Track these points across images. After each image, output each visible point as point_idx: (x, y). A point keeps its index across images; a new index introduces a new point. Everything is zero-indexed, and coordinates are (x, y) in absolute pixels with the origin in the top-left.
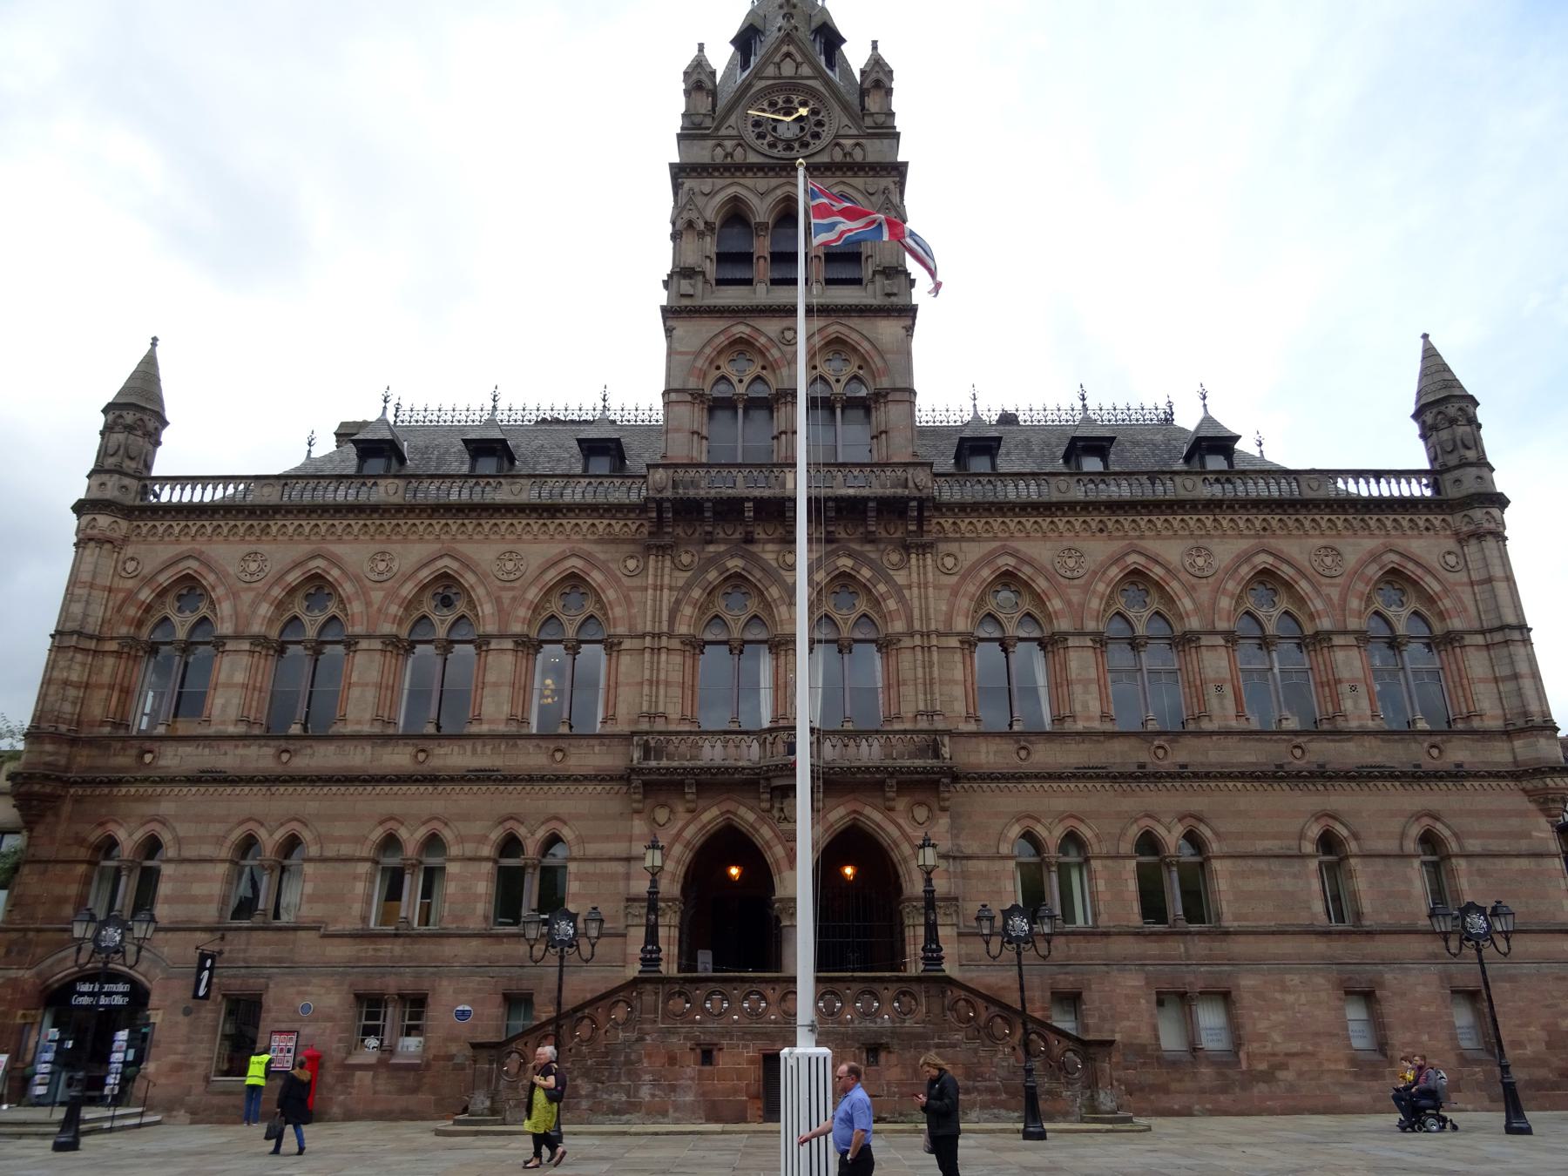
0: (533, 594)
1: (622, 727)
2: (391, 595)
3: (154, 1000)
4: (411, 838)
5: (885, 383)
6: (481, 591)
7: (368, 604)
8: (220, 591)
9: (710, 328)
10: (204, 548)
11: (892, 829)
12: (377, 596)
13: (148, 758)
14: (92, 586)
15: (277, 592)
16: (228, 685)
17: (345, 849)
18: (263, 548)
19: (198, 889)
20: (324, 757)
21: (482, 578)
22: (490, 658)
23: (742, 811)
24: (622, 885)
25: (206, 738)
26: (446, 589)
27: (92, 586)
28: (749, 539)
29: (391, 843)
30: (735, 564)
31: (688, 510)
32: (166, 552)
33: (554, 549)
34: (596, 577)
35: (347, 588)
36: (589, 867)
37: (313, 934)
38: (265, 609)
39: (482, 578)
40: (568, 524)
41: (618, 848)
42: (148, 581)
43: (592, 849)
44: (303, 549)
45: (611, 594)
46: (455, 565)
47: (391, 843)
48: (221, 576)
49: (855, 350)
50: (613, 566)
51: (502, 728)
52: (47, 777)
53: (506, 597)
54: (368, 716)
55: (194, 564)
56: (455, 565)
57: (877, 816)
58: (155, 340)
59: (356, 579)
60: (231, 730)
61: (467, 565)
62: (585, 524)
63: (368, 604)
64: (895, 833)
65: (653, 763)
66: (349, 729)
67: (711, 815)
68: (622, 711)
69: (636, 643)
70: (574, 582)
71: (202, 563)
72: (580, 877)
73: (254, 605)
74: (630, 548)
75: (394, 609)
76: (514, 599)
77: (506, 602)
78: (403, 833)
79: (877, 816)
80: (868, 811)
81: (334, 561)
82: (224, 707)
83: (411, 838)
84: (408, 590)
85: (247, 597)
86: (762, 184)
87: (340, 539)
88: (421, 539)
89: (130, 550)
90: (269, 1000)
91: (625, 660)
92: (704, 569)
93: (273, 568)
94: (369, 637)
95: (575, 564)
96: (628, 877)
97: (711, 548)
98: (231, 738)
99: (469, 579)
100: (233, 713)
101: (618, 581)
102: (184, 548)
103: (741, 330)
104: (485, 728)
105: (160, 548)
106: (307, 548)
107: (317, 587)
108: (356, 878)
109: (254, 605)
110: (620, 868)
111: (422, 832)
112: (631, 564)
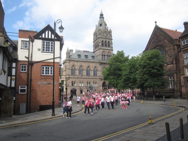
3: (77, 90)
4: (89, 82)
26: (88, 67)
29: (88, 82)
31: (102, 63)
38: (79, 67)
41: (99, 82)
44: (80, 64)
47: (88, 82)
67: (104, 81)
68: (99, 75)
70: (96, 67)
83: (89, 82)
86: (105, 39)
89: (70, 63)
100: (78, 74)
103: (104, 51)
107: (81, 66)
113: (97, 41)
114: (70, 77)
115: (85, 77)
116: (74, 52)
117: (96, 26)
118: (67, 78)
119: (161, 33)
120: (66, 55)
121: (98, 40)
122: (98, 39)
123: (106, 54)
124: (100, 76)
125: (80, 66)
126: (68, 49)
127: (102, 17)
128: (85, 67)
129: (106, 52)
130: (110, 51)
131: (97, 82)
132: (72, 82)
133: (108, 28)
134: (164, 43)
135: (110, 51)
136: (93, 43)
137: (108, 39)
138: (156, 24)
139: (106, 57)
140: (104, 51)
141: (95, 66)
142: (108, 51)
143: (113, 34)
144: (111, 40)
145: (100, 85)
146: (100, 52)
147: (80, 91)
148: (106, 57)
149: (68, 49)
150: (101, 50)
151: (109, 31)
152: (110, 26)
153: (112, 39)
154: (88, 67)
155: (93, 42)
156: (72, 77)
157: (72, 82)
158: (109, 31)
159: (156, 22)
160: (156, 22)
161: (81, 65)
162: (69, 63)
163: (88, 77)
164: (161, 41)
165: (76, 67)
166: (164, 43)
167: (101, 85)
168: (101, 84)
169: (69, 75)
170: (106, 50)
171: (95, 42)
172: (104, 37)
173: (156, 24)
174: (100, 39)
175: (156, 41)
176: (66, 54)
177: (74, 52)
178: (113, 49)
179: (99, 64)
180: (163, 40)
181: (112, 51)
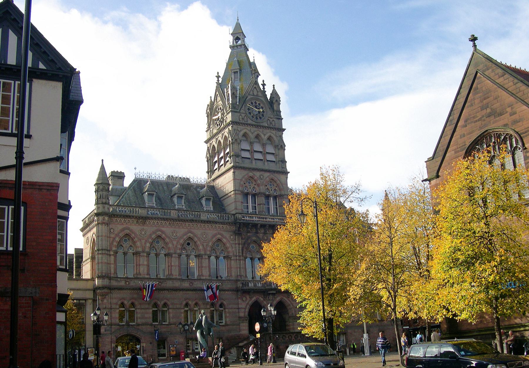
0: (210, 244)
1: (233, 278)
2: (178, 242)
5: (283, 193)
6: (199, 243)
7: (173, 245)
8: (136, 239)
9: (244, 173)
10: (130, 226)
11: (288, 301)
12: (175, 243)
13: (127, 283)
14: (102, 236)
15: (150, 240)
16: (143, 265)
17: (178, 306)
18: (145, 228)
19: (146, 316)
20: (169, 284)
21: (199, 239)
22: (203, 260)
23: (260, 298)
24: (237, 314)
25: (141, 278)
26: (189, 241)
27: (102, 236)
28: (257, 233)
29: (187, 305)
30: (254, 238)
32: (120, 227)
33: (215, 232)
34: (224, 240)
35: (167, 240)
36: (231, 310)
37: (174, 326)
38: (148, 245)
39: (199, 239)
40: (217, 225)
42: (117, 235)
43: (230, 306)
44: (154, 229)
45: (228, 245)
46: (192, 235)
47: (187, 305)
48: (135, 234)
49: (275, 182)
50: (228, 237)
51: (208, 278)
52: (106, 288)
53: (205, 244)
54: (178, 274)
55: (129, 231)
56: (192, 235)
57: (286, 299)
58: (103, 160)
59: (169, 238)
60: (146, 276)
61: (196, 236)
62: (221, 226)
63: (173, 245)
64: (289, 303)
65: (245, 288)
66: (174, 277)
67: (254, 299)
68: (233, 274)
69: (235, 258)
71: (130, 231)
72: (229, 313)
73: (145, 243)
74: (231, 233)
75: (179, 246)
76: (207, 245)
77: (205, 246)
78: (190, 302)
79: (286, 299)
80: (284, 298)
81: (163, 232)
82: (143, 271)
84: (182, 241)
85: (143, 241)
86: (253, 129)
87: (164, 227)
88: (183, 228)
89: (111, 226)
90: (168, 339)
91: (233, 262)
92: (248, 240)
93: (148, 233)
94: (175, 253)
95: (219, 236)
96: (239, 312)
97: (249, 234)
98: (147, 278)
99: (196, 239)
100: (146, 271)
101: (229, 242)
102: (125, 226)
103: (251, 174)
104: (204, 278)
105: (118, 226)
106: (156, 228)
108: (181, 313)
109: (145, 243)
110: (237, 310)
111: (194, 302)
112: (232, 237)
113: (220, 137)
114: (114, 283)
115: (177, 284)
116: (127, 182)
117: (218, 77)
118: (99, 288)
119: (501, 79)
120: (97, 191)
121: (226, 132)
122: (224, 128)
123: (262, 189)
124: (237, 281)
125: (154, 236)
126: (103, 168)
127: (240, 42)
128: (175, 243)
129: (259, 182)
130: (276, 176)
131: (225, 302)
132: (123, 305)
133: (264, 85)
134: (515, 122)
135: (276, 175)
136: (205, 146)
137: (268, 128)
138: (475, 46)
139: (261, 200)
140: (252, 177)
141: (215, 235)
142: (267, 174)
143: (284, 108)
144: (280, 133)
145: (239, 317)
146: (235, 179)
147: (156, 344)
148: (261, 200)
149: (103, 168)
150: (237, 172)
151: (269, 97)
152: (269, 79)
153: (284, 130)
154: (188, 244)
155: (206, 142)
156: (123, 283)
157: (123, 305)
158: (269, 97)
159: (474, 39)
160: (474, 39)
161: (159, 233)
162: (107, 224)
163: (186, 285)
164: (501, 114)
165: (138, 244)
166: (515, 122)
167: (242, 315)
168: (244, 313)
169: (110, 278)
170: (258, 174)
171: (214, 142)
172: (250, 122)
173: (475, 46)
174: (235, 127)
175: (479, 116)
176: (94, 188)
177: (127, 182)
178: (289, 167)
179: (233, 228)
180: (509, 110)
181: (282, 177)
